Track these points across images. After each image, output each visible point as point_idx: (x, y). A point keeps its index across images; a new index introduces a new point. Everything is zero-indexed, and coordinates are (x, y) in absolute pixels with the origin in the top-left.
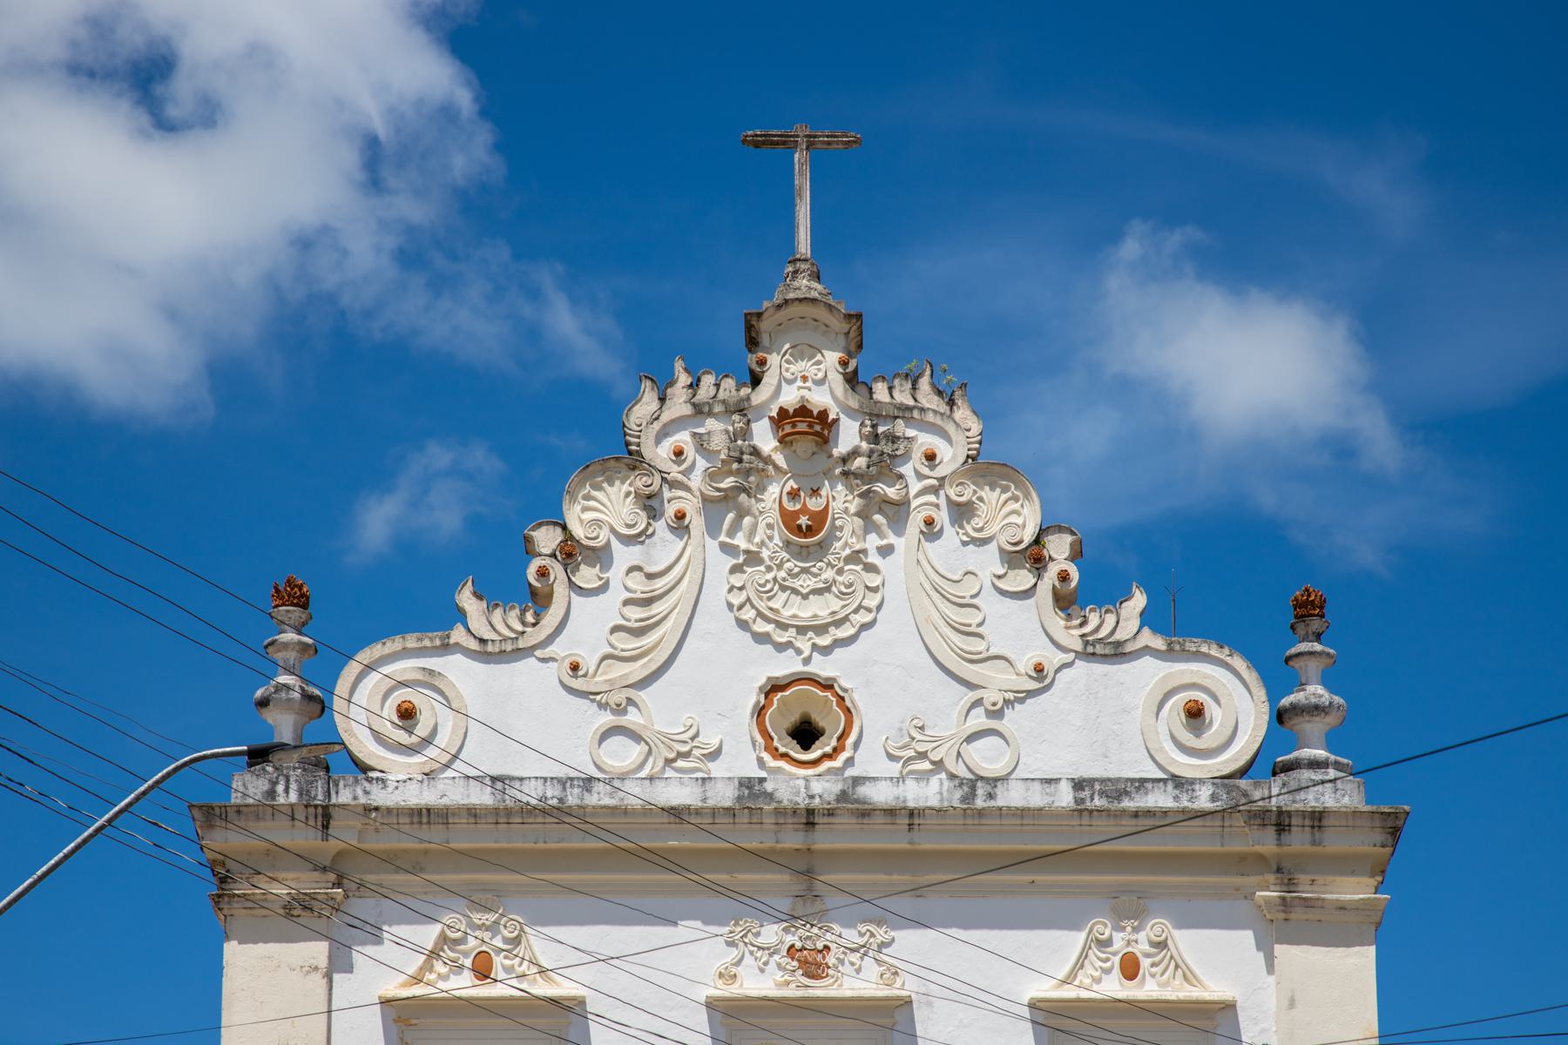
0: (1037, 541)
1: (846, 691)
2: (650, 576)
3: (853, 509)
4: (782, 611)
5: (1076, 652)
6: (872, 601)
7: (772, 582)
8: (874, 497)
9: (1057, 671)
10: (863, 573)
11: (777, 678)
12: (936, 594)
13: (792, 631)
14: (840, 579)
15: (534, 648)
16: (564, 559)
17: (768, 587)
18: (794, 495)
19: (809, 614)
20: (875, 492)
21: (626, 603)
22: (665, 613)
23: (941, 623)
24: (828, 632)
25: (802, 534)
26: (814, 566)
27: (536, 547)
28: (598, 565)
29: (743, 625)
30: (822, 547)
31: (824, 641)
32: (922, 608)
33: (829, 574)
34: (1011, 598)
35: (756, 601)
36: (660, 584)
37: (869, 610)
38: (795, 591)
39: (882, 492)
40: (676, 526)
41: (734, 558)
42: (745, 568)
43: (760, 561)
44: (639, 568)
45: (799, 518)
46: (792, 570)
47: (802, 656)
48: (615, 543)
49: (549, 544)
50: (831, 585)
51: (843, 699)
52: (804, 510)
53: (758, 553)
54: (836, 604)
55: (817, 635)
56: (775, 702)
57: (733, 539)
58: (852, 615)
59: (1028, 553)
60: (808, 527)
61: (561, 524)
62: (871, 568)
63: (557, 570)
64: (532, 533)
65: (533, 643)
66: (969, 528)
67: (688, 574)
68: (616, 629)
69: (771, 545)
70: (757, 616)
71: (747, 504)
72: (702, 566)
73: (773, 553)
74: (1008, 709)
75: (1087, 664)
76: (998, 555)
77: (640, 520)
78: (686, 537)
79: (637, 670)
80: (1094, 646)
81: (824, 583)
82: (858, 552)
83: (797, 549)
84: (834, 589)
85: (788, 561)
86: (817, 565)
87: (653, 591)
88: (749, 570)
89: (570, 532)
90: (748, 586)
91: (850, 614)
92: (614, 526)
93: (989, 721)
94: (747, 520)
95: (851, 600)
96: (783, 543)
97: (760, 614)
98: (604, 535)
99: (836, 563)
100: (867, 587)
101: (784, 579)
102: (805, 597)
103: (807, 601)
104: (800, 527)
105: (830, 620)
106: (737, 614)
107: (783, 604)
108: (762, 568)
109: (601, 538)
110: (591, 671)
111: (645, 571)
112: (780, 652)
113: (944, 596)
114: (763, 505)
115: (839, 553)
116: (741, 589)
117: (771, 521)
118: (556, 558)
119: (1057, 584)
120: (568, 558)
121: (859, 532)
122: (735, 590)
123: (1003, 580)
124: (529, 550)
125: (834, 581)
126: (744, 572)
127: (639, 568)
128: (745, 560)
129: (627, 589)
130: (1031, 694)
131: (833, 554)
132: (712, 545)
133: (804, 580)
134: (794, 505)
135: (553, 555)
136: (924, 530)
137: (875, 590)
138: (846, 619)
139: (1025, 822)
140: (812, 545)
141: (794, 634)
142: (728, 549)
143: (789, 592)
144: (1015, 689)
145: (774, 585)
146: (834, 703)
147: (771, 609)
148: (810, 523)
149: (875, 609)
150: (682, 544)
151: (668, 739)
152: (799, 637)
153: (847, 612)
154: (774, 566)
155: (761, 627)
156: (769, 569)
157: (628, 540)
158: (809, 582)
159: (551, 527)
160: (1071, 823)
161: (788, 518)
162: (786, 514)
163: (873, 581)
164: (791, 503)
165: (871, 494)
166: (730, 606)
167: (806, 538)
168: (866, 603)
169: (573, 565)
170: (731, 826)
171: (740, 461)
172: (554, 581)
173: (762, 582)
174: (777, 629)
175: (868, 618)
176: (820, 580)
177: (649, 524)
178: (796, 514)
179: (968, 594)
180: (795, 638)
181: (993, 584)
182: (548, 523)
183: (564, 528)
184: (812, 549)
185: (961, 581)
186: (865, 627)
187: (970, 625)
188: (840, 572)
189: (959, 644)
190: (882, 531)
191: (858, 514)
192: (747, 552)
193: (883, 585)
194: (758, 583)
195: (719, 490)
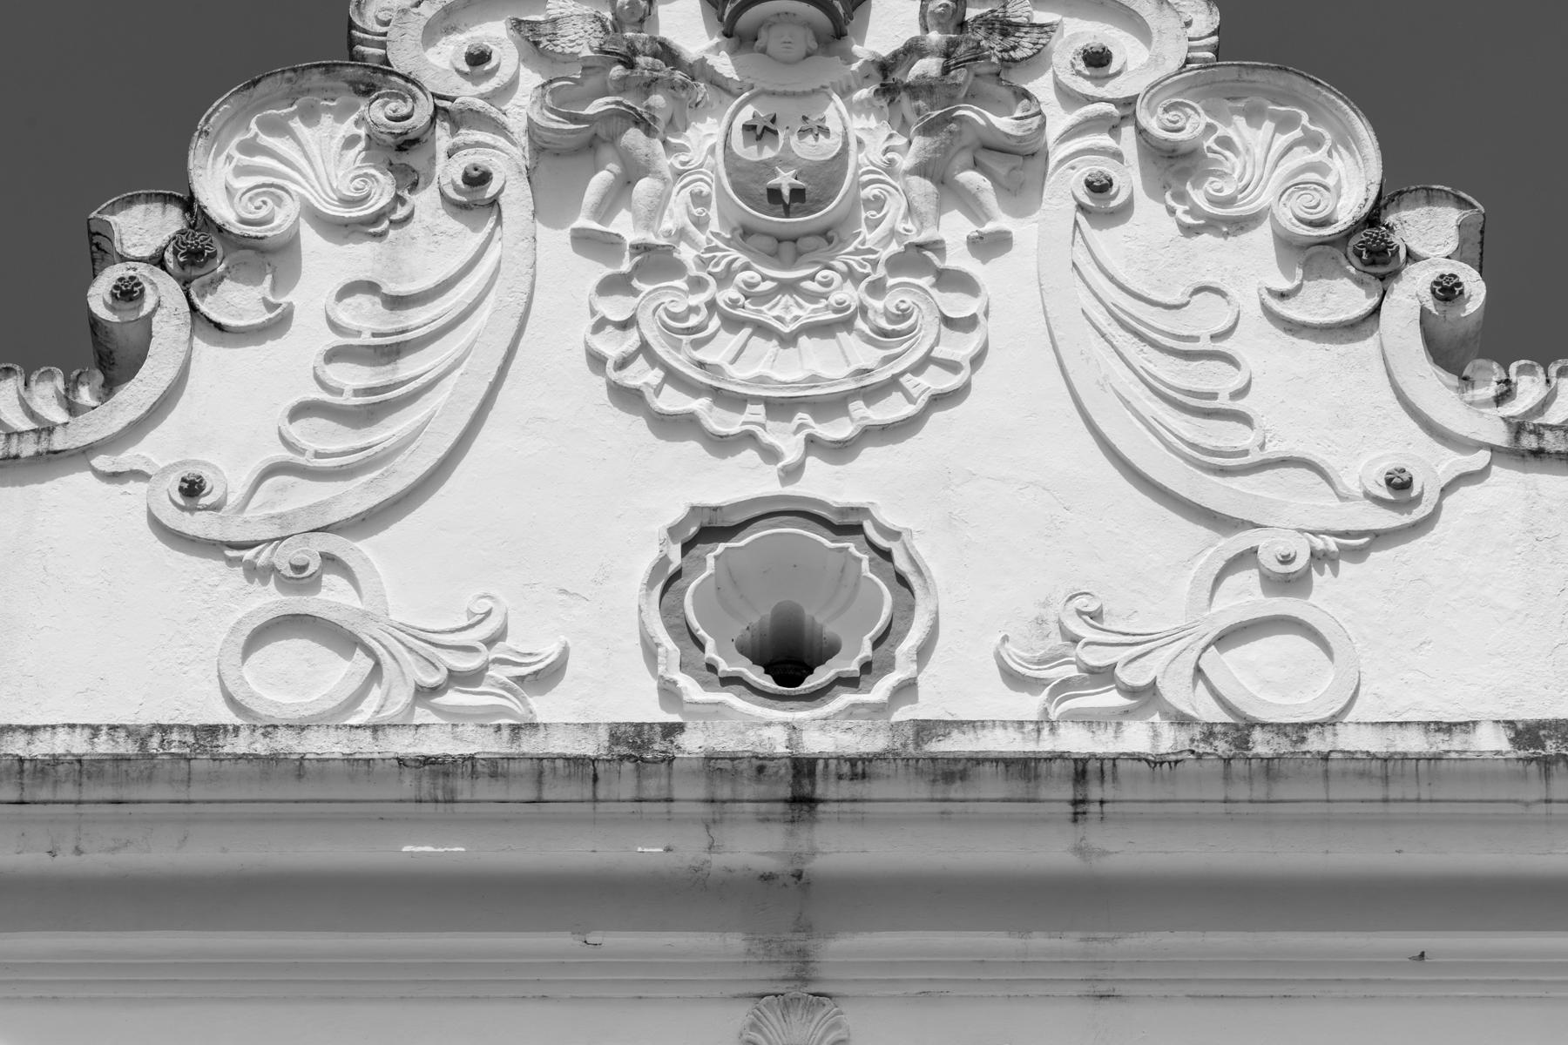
0: (1372, 219)
1: (895, 535)
2: (397, 302)
3: (905, 162)
4: (732, 370)
5: (1493, 449)
6: (959, 347)
7: (704, 312)
8: (960, 133)
9: (1445, 491)
10: (934, 292)
11: (715, 509)
12: (1122, 332)
13: (756, 412)
14: (876, 304)
15: (88, 451)
16: (182, 266)
17: (693, 321)
18: (759, 132)
19: (798, 375)
20: (961, 119)
21: (333, 355)
22: (430, 376)
23: (1139, 395)
24: (847, 413)
25: (781, 209)
26: (812, 278)
27: (117, 244)
28: (268, 278)
29: (628, 398)
30: (830, 241)
31: (838, 430)
32: (1088, 360)
33: (849, 294)
34: (1316, 339)
35: (661, 350)
36: (418, 319)
37: (952, 367)
38: (763, 330)
39: (982, 122)
40: (464, 199)
41: (607, 266)
42: (636, 283)
43: (677, 269)
44: (371, 287)
45: (775, 174)
46: (756, 285)
47: (780, 465)
48: (310, 239)
49: (148, 239)
50: (853, 316)
51: (887, 555)
52: (785, 161)
53: (668, 250)
54: (867, 356)
55: (817, 420)
56: (710, 561)
57: (607, 225)
58: (908, 376)
59: (1354, 241)
60: (798, 194)
61: (179, 199)
62: (960, 282)
63: (163, 291)
64: (107, 217)
65: (90, 439)
66: (1198, 197)
67: (491, 297)
68: (302, 411)
69: (701, 238)
70: (664, 380)
71: (644, 150)
72: (528, 279)
73: (708, 250)
74: (1321, 573)
75: (1519, 476)
76: (1274, 254)
77: (376, 191)
78: (490, 224)
79: (354, 497)
80: (1540, 436)
81: (836, 311)
82: (920, 246)
83: (768, 243)
84: (859, 323)
85: (747, 267)
86: (818, 277)
87: (403, 332)
88: (645, 288)
89: (202, 210)
90: (645, 319)
91: (903, 373)
92: (313, 201)
93: (1275, 600)
94: (644, 186)
95: (905, 346)
96: (734, 230)
97: (673, 377)
98: (283, 218)
99: (868, 270)
100: (947, 321)
101: (734, 303)
102: (788, 341)
103: (791, 350)
104: (774, 194)
105: (852, 385)
106: (614, 376)
107: (732, 356)
108: (680, 283)
109: (276, 222)
110: (232, 500)
111: (385, 290)
112: (723, 457)
113: (1136, 334)
114: (683, 158)
115: (875, 252)
116: (624, 326)
117: (706, 189)
118: (164, 268)
119: (1430, 305)
120: (193, 264)
121: (925, 206)
122: (609, 329)
123: (1291, 302)
124: (99, 249)
125: (863, 310)
126: (635, 292)
127: (371, 287)
128: (636, 266)
129: (334, 326)
130: (1381, 538)
131: (857, 252)
132: (555, 242)
133: (787, 308)
134: (760, 151)
135: (158, 261)
136: (1086, 200)
137: (969, 323)
138: (893, 384)
139: (1395, 792)
140: (808, 235)
141: (761, 418)
142: (586, 242)
143: (747, 331)
144: (1342, 528)
145: (710, 316)
146: (865, 565)
147: (701, 365)
148: (799, 183)
149: (966, 364)
150: (480, 237)
151: (426, 642)
152: (770, 424)
153: (896, 371)
154: (711, 280)
155: (672, 401)
156: (697, 284)
157: (342, 230)
158: (796, 311)
159: (156, 208)
160: (1520, 797)
161: (746, 180)
162: (738, 170)
163: (958, 305)
164: (755, 148)
165: (953, 126)
166: (596, 361)
167: (787, 215)
168: (940, 352)
169: (207, 278)
170: (587, 807)
171: (629, 64)
172: (154, 311)
173: (679, 308)
174: (716, 409)
175: (950, 382)
176: (827, 307)
177: (399, 199)
178: (768, 167)
179: (1205, 334)
180: (763, 426)
181: (1263, 305)
182: (149, 198)
183: (189, 204)
184: (804, 243)
185: (1188, 303)
186: (940, 400)
187: (1213, 396)
188: (877, 289)
189: (1188, 436)
190: (980, 205)
191: (921, 170)
192: (639, 248)
193: (986, 314)
194: (666, 310)
195: (575, 119)
